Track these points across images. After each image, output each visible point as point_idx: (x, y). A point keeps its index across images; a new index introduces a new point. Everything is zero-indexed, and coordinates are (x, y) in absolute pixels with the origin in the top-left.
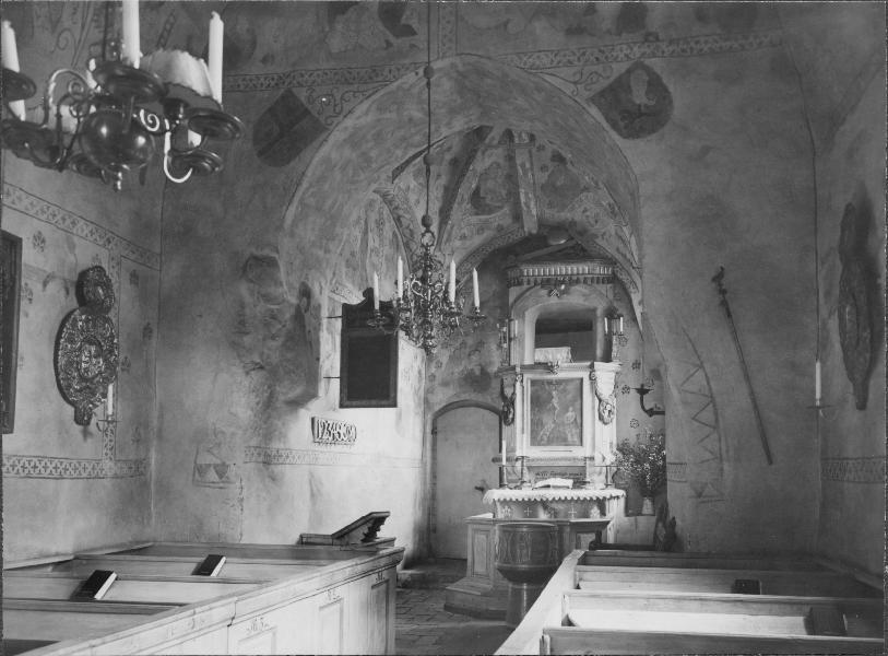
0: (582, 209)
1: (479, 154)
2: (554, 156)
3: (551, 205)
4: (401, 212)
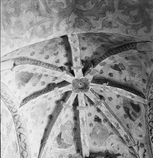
0: (111, 143)
1: (63, 109)
2: (95, 118)
3: (95, 143)
4: (21, 131)
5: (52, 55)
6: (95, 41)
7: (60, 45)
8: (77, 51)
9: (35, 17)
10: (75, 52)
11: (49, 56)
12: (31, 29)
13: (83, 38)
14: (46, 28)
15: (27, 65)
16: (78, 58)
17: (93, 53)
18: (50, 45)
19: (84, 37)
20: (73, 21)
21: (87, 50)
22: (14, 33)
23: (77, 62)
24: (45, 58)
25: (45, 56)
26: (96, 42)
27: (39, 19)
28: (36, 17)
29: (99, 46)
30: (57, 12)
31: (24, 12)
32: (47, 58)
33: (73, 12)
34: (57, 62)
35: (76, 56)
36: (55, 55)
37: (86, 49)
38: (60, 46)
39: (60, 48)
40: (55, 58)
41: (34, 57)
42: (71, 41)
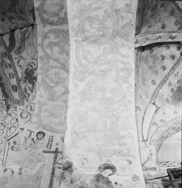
5: (163, 63)
6: (155, 14)
7: (152, 53)
8: (161, 36)
9: (111, 76)
10: (163, 38)
11: (163, 66)
12: (120, 81)
13: (149, 27)
14: (123, 67)
15: (161, 91)
16: (172, 35)
17: (171, 15)
18: (150, 64)
19: (148, 26)
20: (122, 40)
21: (165, 23)
22: (119, 98)
23: (177, 36)
24: (164, 70)
25: (162, 70)
26: (157, 13)
27: (114, 72)
28: (112, 75)
29: (163, 9)
30: (111, 55)
31: (104, 84)
32: (164, 68)
33: (114, 40)
34: (174, 58)
35: (168, 38)
36: (164, 59)
37: (165, 24)
38: (154, 53)
39: (156, 53)
40: (168, 59)
41: (158, 82)
42: (146, 43)
